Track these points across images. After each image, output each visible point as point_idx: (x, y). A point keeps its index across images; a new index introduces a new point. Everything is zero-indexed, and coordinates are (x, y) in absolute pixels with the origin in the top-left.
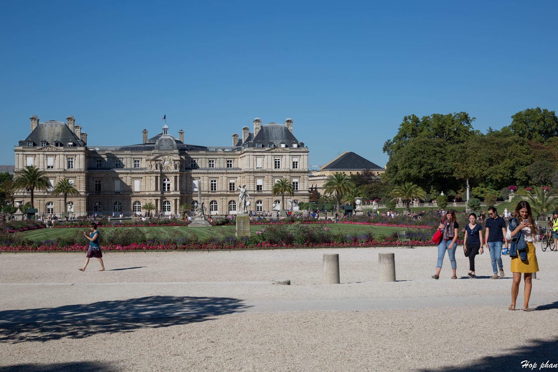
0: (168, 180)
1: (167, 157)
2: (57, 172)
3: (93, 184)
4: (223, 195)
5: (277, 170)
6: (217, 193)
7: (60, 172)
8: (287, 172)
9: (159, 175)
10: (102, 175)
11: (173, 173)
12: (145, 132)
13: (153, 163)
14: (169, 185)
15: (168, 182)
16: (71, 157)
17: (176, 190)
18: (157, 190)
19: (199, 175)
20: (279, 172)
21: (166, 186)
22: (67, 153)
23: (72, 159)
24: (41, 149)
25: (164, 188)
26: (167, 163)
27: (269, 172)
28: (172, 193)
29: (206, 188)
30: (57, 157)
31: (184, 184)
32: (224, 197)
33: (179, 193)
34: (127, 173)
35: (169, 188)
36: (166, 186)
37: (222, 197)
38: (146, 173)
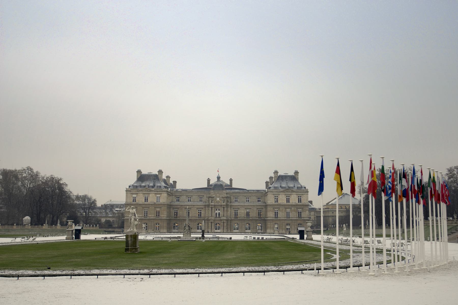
0: (219, 210)
1: (218, 195)
2: (149, 204)
3: (173, 211)
4: (254, 220)
5: (288, 204)
7: (152, 205)
8: (294, 205)
9: (213, 206)
10: (178, 207)
11: (221, 205)
12: (209, 180)
13: (210, 199)
17: (224, 216)
18: (212, 216)
19: (239, 207)
20: (289, 205)
26: (218, 199)
27: (282, 205)
28: (222, 218)
29: (243, 215)
30: (151, 195)
31: (229, 213)
33: (225, 218)
34: (194, 206)
38: (205, 205)
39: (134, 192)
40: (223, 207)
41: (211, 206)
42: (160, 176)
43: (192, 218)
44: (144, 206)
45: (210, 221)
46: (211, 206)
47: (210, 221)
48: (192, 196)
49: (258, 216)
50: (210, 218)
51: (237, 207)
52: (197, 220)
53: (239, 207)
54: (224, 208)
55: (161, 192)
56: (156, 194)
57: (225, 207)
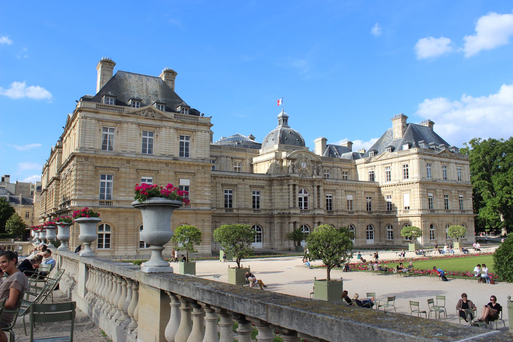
0: (306, 192)
6: (355, 214)
7: (167, 164)
11: (312, 181)
14: (306, 198)
15: (306, 195)
16: (185, 134)
19: (335, 187)
21: (303, 202)
22: (179, 126)
23: (188, 138)
24: (134, 113)
25: (300, 204)
26: (304, 165)
28: (311, 212)
30: (163, 133)
32: (363, 219)
34: (244, 179)
35: (306, 205)
36: (303, 202)
37: (360, 219)
39: (108, 117)
40: (316, 184)
41: (292, 182)
42: (170, 84)
43: (240, 212)
44: (141, 166)
45: (293, 220)
46: (292, 182)
47: (293, 220)
48: (217, 157)
49: (366, 210)
50: (292, 211)
51: (331, 187)
52: (251, 216)
53: (335, 187)
54: (318, 187)
55: (193, 127)
56: (177, 129)
57: (321, 184)
